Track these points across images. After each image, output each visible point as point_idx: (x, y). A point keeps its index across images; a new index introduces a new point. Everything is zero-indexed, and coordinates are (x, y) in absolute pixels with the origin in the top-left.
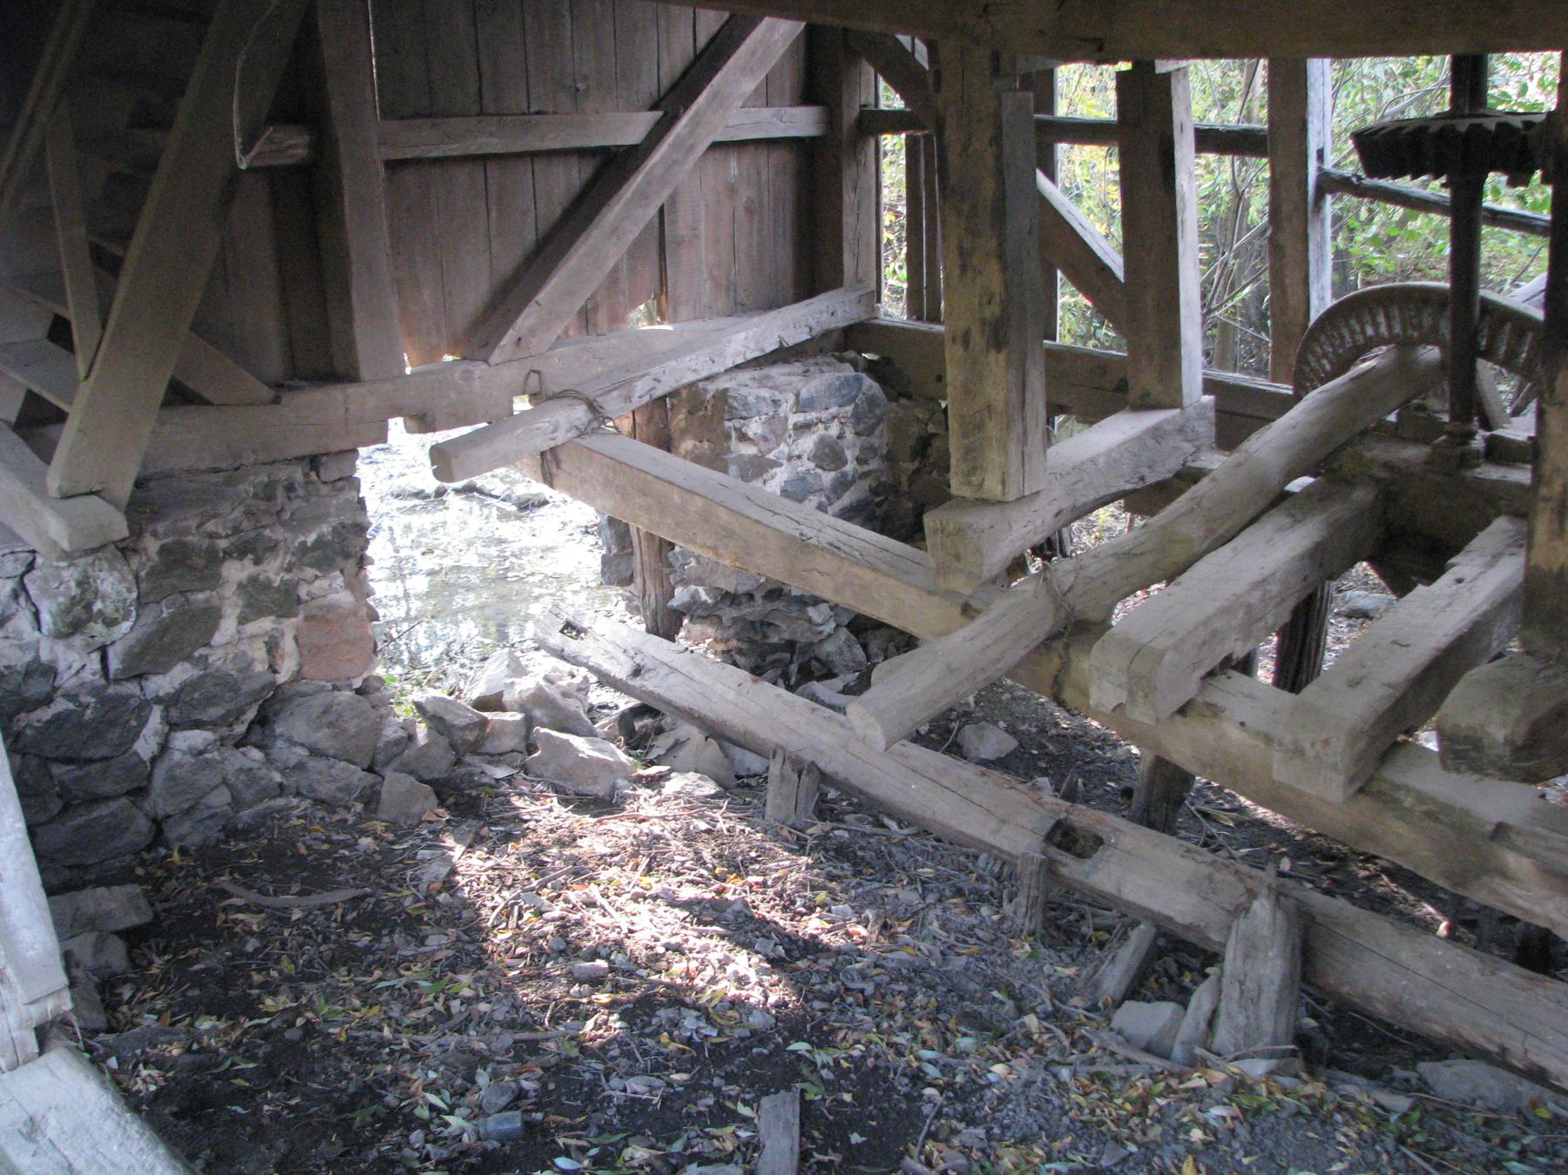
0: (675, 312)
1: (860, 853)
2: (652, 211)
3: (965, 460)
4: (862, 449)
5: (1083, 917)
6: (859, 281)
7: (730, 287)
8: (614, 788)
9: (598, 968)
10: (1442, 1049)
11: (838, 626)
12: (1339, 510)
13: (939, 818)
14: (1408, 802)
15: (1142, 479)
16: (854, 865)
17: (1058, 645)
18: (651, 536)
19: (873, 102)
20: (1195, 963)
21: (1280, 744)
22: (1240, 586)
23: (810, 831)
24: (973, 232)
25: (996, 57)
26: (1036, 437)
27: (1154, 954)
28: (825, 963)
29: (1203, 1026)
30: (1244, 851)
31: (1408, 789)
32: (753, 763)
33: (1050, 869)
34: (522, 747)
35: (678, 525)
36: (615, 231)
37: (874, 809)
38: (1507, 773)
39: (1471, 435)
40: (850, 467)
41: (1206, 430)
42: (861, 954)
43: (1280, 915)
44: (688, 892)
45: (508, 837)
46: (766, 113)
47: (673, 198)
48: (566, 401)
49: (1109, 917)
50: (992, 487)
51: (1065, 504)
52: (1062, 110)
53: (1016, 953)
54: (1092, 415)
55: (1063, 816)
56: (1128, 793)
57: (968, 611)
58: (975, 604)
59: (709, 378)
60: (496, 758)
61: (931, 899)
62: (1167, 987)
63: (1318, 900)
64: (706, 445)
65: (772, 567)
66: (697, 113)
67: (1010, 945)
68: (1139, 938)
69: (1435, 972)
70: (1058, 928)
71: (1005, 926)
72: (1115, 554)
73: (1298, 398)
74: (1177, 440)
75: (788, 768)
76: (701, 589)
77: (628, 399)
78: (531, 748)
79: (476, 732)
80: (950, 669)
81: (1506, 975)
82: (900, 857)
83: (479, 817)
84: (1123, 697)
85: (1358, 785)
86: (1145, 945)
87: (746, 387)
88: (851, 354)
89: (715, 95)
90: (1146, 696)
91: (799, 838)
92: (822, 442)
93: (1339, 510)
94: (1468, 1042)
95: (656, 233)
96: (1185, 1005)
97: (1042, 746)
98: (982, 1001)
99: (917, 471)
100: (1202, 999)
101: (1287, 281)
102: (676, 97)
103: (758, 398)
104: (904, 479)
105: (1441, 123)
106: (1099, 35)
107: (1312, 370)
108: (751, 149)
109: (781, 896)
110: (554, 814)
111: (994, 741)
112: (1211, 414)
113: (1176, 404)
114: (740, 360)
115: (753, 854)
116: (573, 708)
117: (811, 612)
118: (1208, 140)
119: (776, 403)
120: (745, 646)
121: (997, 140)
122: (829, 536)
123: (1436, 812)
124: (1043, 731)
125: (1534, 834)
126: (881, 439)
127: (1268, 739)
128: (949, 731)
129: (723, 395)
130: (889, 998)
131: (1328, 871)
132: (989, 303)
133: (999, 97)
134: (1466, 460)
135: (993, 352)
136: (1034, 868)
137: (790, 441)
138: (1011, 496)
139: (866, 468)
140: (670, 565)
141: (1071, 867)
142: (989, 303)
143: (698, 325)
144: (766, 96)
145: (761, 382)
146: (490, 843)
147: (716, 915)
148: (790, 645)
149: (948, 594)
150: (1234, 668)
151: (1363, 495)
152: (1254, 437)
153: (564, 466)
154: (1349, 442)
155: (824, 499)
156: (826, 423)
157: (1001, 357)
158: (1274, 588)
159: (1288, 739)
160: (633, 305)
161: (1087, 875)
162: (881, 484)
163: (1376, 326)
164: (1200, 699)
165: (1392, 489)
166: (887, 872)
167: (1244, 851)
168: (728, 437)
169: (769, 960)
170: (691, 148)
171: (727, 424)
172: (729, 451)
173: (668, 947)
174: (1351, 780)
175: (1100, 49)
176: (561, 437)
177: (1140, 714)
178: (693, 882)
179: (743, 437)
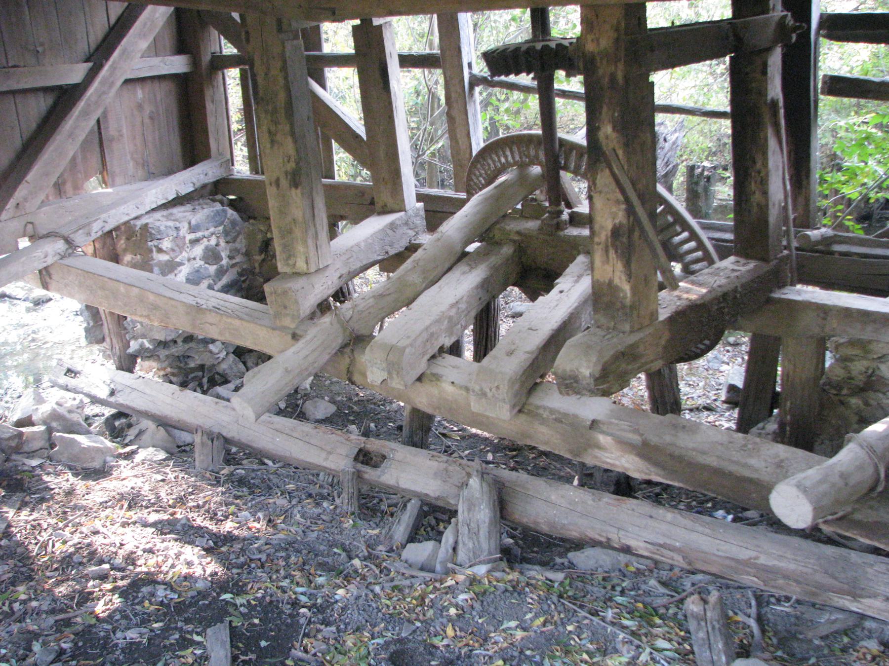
0: (113, 181)
1: (252, 481)
2: (93, 122)
3: (284, 252)
4: (231, 251)
5: (381, 500)
6: (221, 154)
7: (144, 164)
8: (105, 462)
9: (104, 570)
10: (578, 545)
11: (227, 354)
12: (495, 260)
13: (294, 455)
14: (545, 415)
15: (387, 253)
16: (249, 488)
17: (348, 350)
18: (112, 314)
19: (218, 50)
20: (445, 517)
21: (473, 391)
22: (444, 307)
23: (222, 472)
25: (279, 22)
26: (324, 233)
27: (422, 515)
28: (237, 546)
29: (451, 551)
30: (467, 452)
31: (545, 408)
32: (186, 437)
33: (358, 476)
34: (47, 445)
35: (125, 305)
36: (71, 135)
37: (258, 456)
38: (593, 393)
39: (561, 212)
40: (225, 262)
41: (421, 222)
42: (257, 538)
43: (484, 485)
44: (153, 517)
45: (43, 500)
46: (156, 61)
47: (105, 114)
48: (49, 239)
49: (395, 499)
50: (301, 265)
51: (344, 271)
53: (346, 525)
54: (357, 219)
55: (362, 445)
56: (400, 428)
57: (295, 337)
58: (298, 332)
59: (136, 218)
60: (31, 454)
61: (294, 502)
62: (431, 534)
63: (505, 474)
64: (139, 257)
65: (184, 325)
66: (114, 63)
67: (341, 522)
68: (413, 507)
69: (570, 504)
70: (368, 508)
71: (338, 511)
72: (374, 297)
73: (468, 200)
74: (405, 229)
75: (205, 437)
76: (145, 341)
77: (89, 234)
78: (52, 446)
79: (16, 440)
80: (286, 370)
81: (605, 500)
82: (275, 480)
83: (24, 491)
84: (385, 375)
85: (517, 409)
86: (416, 512)
87: (158, 221)
88: (219, 197)
89: (124, 51)
90: (398, 373)
91: (216, 477)
92: (207, 249)
93: (495, 260)
94: (591, 539)
95: (97, 134)
96: (440, 542)
97: (350, 408)
98: (328, 555)
99: (263, 260)
100: (448, 537)
101: (459, 136)
102: (100, 54)
103: (166, 227)
104: (257, 265)
105: (527, 45)
107: (475, 184)
108: (149, 82)
109: (208, 512)
110: (69, 483)
111: (323, 408)
112: (423, 213)
113: (402, 209)
114: (154, 206)
115: (190, 490)
116: (75, 419)
117: (211, 347)
118: (408, 61)
119: (177, 229)
120: (175, 371)
121: (284, 68)
122: (213, 302)
123: (561, 418)
124: (350, 399)
125: (611, 423)
126: (241, 244)
127: (467, 389)
128: (298, 406)
129: (145, 226)
130: (275, 561)
131: (513, 457)
132: (289, 162)
133: (283, 43)
134: (559, 226)
135: (293, 190)
136: (350, 477)
137: (188, 250)
138: (312, 270)
139: (234, 261)
140: (125, 329)
141: (370, 474)
143: (127, 187)
144: (155, 50)
145: (168, 218)
146: (31, 505)
147: (171, 528)
148: (202, 367)
149: (283, 329)
150: (445, 352)
151: (507, 250)
152: (444, 224)
153: (54, 277)
154: (497, 222)
155: (211, 282)
156: (208, 238)
157: (299, 191)
158: (463, 306)
159: (477, 388)
160: (87, 177)
161: (379, 477)
162: (243, 270)
163: (506, 157)
164: (428, 372)
165: (522, 246)
166: (269, 489)
167: (467, 452)
168: (151, 251)
169: (204, 550)
170: (113, 83)
171: (150, 244)
172: (153, 260)
173: (145, 551)
174: (514, 406)
175: (334, 13)
176: (50, 261)
177: (396, 384)
178: (156, 511)
179: (160, 250)
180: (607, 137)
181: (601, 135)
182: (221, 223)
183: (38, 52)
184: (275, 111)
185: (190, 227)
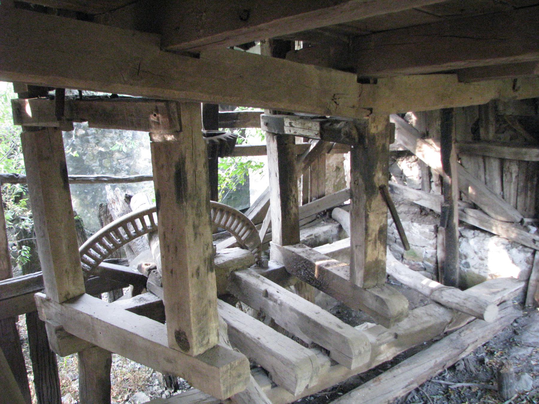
24: (199, 215)
106: (371, 106)
132: (207, 249)
142: (207, 249)
180: (379, 180)
181: (375, 179)
184: (199, 205)
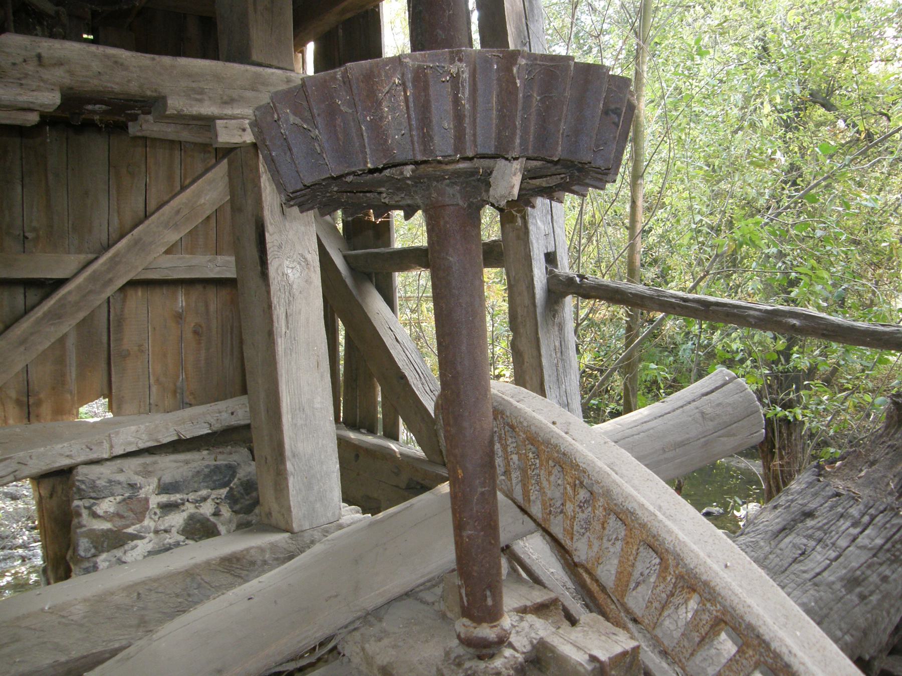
52: (398, 243)
89: (137, 242)
108: (200, 288)
170: (111, 281)
171: (76, 503)
179: (95, 515)
182: (224, 486)
183: (26, 238)
185: (159, 486)
